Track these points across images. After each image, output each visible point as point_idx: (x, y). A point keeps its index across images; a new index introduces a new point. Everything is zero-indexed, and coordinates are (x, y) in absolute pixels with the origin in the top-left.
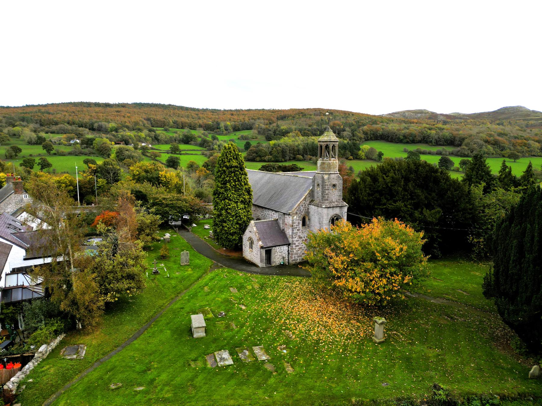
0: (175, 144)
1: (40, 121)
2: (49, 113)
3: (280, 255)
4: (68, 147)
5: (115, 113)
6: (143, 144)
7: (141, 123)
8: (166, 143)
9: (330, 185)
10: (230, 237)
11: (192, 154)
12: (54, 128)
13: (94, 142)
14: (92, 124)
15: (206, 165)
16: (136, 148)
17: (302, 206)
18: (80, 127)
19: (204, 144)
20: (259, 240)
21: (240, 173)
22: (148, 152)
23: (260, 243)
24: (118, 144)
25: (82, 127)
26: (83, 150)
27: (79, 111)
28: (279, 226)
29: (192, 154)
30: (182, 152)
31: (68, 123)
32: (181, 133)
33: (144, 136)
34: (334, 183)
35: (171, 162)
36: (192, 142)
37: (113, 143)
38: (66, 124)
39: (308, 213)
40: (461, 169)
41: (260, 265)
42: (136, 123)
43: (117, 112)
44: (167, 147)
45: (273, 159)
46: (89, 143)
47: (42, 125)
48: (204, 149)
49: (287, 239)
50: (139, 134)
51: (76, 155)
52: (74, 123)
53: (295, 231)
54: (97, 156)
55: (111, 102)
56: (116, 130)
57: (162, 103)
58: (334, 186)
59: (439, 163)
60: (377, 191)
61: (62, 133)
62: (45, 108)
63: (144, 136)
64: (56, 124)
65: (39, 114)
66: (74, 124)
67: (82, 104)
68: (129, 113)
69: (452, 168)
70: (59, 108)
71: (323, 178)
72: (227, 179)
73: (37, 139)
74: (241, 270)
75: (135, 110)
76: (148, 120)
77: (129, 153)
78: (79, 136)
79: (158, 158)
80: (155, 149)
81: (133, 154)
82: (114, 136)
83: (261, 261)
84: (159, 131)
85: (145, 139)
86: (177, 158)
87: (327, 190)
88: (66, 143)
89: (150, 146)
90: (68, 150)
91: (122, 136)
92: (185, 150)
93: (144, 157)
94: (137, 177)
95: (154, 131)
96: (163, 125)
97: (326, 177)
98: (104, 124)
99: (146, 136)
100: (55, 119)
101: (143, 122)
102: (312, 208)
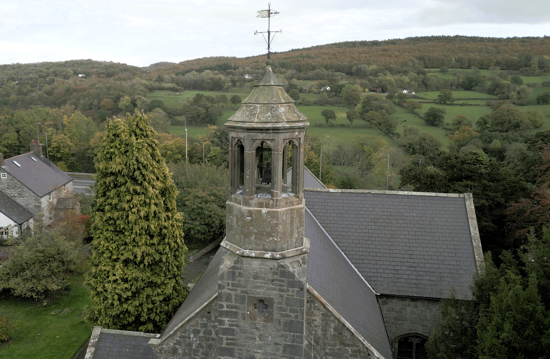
0: (447, 91)
1: (299, 67)
2: (309, 57)
4: (316, 95)
5: (381, 53)
6: (405, 92)
7: (410, 63)
8: (438, 89)
9: (242, 299)
11: (471, 105)
12: (310, 74)
13: (343, 89)
14: (351, 67)
15: (482, 123)
16: (390, 97)
17: (196, 332)
18: (336, 72)
19: (494, 89)
21: (128, 190)
22: (406, 102)
24: (373, 91)
25: (339, 71)
26: (329, 99)
27: (340, 53)
29: (471, 105)
30: (456, 102)
31: (326, 68)
32: (462, 74)
33: (408, 80)
34: (261, 293)
35: (432, 115)
36: (477, 88)
37: (367, 90)
38: (323, 69)
42: (404, 64)
43: (384, 50)
44: (434, 95)
46: (337, 90)
47: (300, 71)
48: (494, 97)
50: (402, 78)
51: (322, 105)
52: (331, 67)
54: (343, 107)
55: (380, 39)
56: (375, 74)
57: (446, 35)
58: (263, 304)
61: (317, 80)
62: (308, 52)
63: (408, 80)
64: (314, 68)
65: (300, 59)
66: (331, 68)
67: (347, 44)
68: (399, 51)
70: (322, 51)
73: (288, 86)
75: (407, 47)
76: (421, 58)
77: (378, 104)
78: (332, 81)
79: (416, 110)
80: (418, 98)
81: (383, 104)
82: (370, 81)
84: (433, 75)
85: (409, 84)
86: (440, 111)
87: (227, 314)
88: (316, 90)
89: (414, 93)
90: (312, 98)
91: (380, 81)
92: (462, 99)
93: (397, 108)
95: (424, 73)
96: (441, 65)
98: (364, 66)
99: (411, 80)
100: (313, 64)
101: (413, 61)
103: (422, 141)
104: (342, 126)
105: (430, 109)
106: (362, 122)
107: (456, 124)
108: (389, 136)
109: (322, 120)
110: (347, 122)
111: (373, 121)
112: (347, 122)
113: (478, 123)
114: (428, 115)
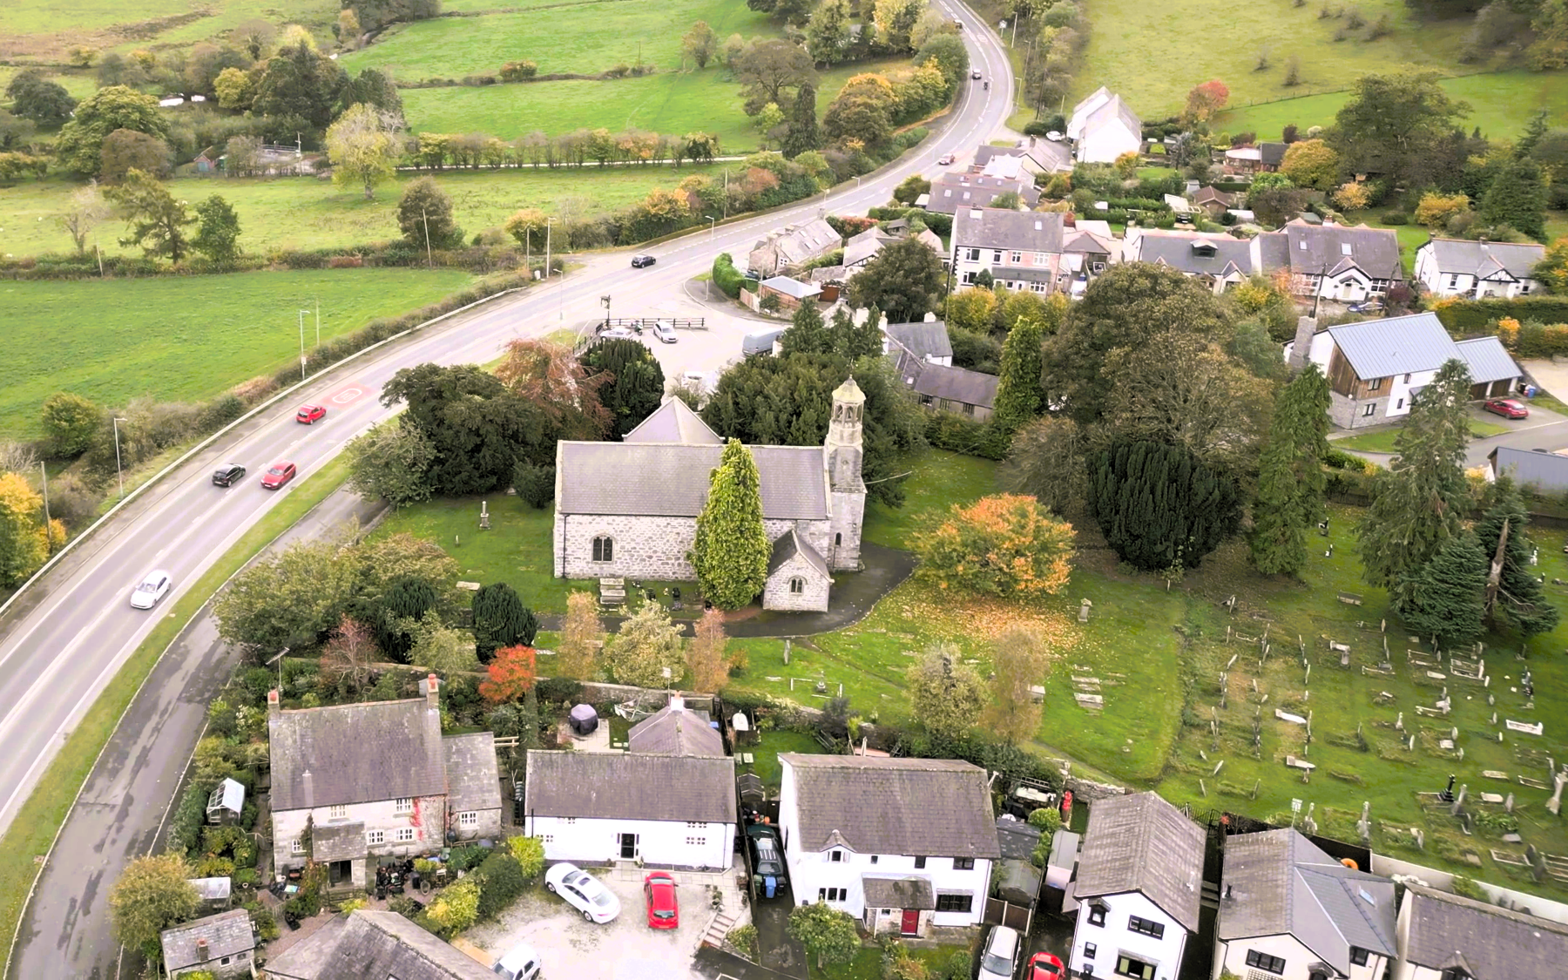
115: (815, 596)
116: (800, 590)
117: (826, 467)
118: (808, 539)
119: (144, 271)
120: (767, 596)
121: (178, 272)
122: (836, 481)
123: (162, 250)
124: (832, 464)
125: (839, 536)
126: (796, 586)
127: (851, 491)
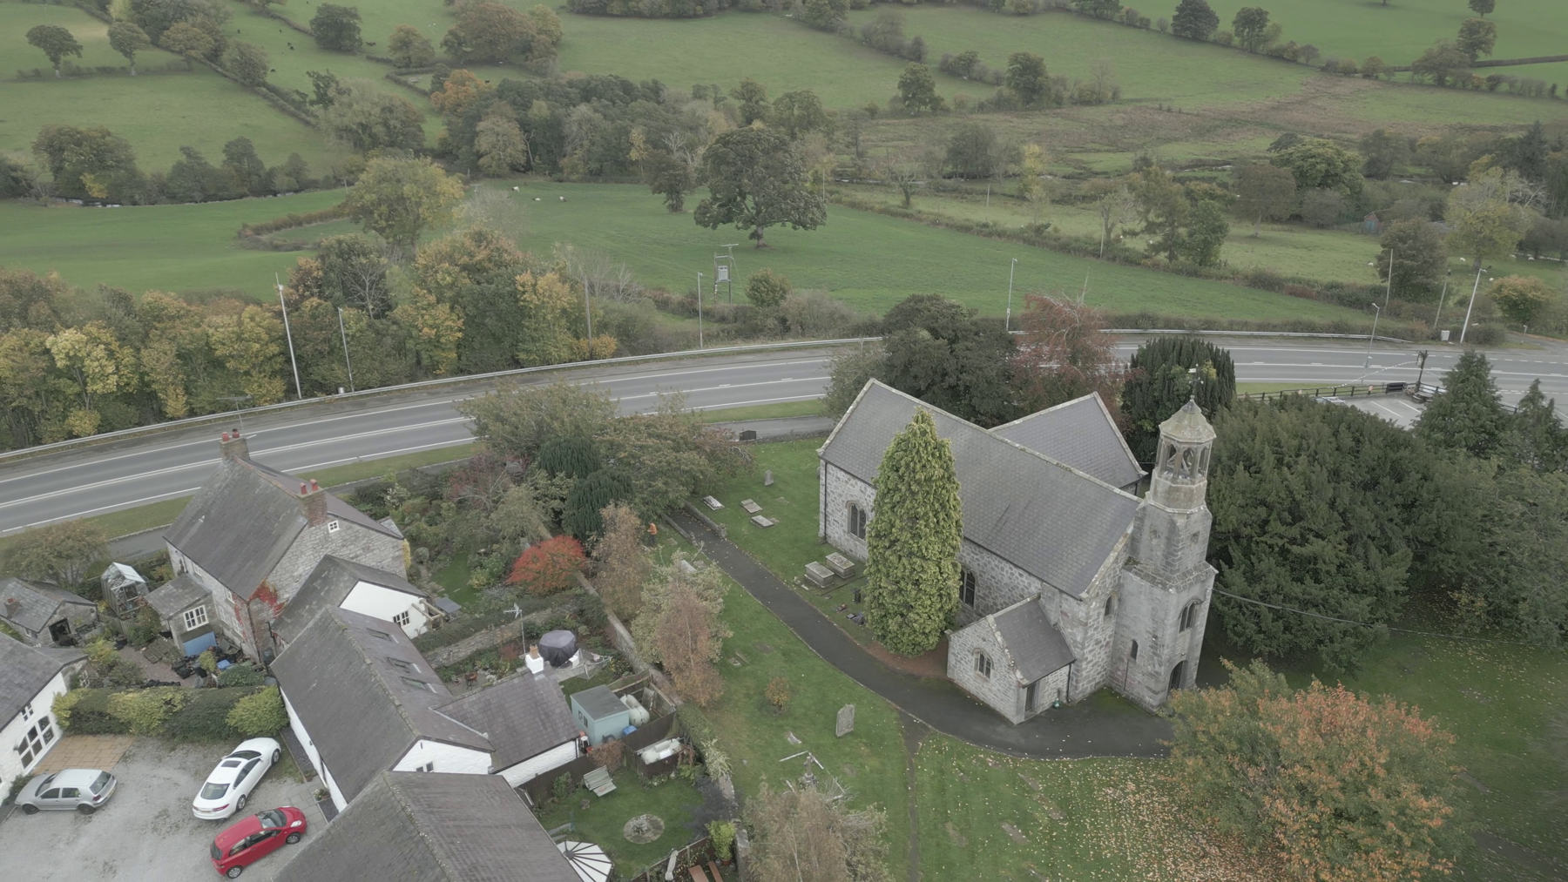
3: (1053, 688)
10: (921, 638)
20: (1013, 668)
23: (1019, 675)
28: (1044, 617)
39: (1119, 586)
40: (1236, 41)
41: (1016, 719)
45: (666, 9)
49: (1068, 648)
53: (1090, 632)
59: (1175, 18)
60: (1263, 503)
69: (1211, 37)
71: (1173, 523)
72: (921, 511)
74: (980, 740)
83: (1018, 713)
94: (449, 294)
97: (1180, 522)
102: (1133, 581)
103: (388, 115)
104: (106, 72)
105: (320, 10)
106: (160, 57)
107: (400, 48)
108: (257, 93)
109: (39, 58)
110: (118, 59)
111: (193, 53)
112: (118, 59)
113: (445, 43)
114: (319, 23)
115: (1001, 692)
116: (988, 671)
117: (1130, 531)
118: (1053, 617)
119: (1131, 260)
120: (951, 659)
121: (1166, 269)
122: (1143, 555)
123: (1156, 249)
124: (1138, 529)
125: (1135, 645)
126: (984, 665)
127: (1153, 581)
